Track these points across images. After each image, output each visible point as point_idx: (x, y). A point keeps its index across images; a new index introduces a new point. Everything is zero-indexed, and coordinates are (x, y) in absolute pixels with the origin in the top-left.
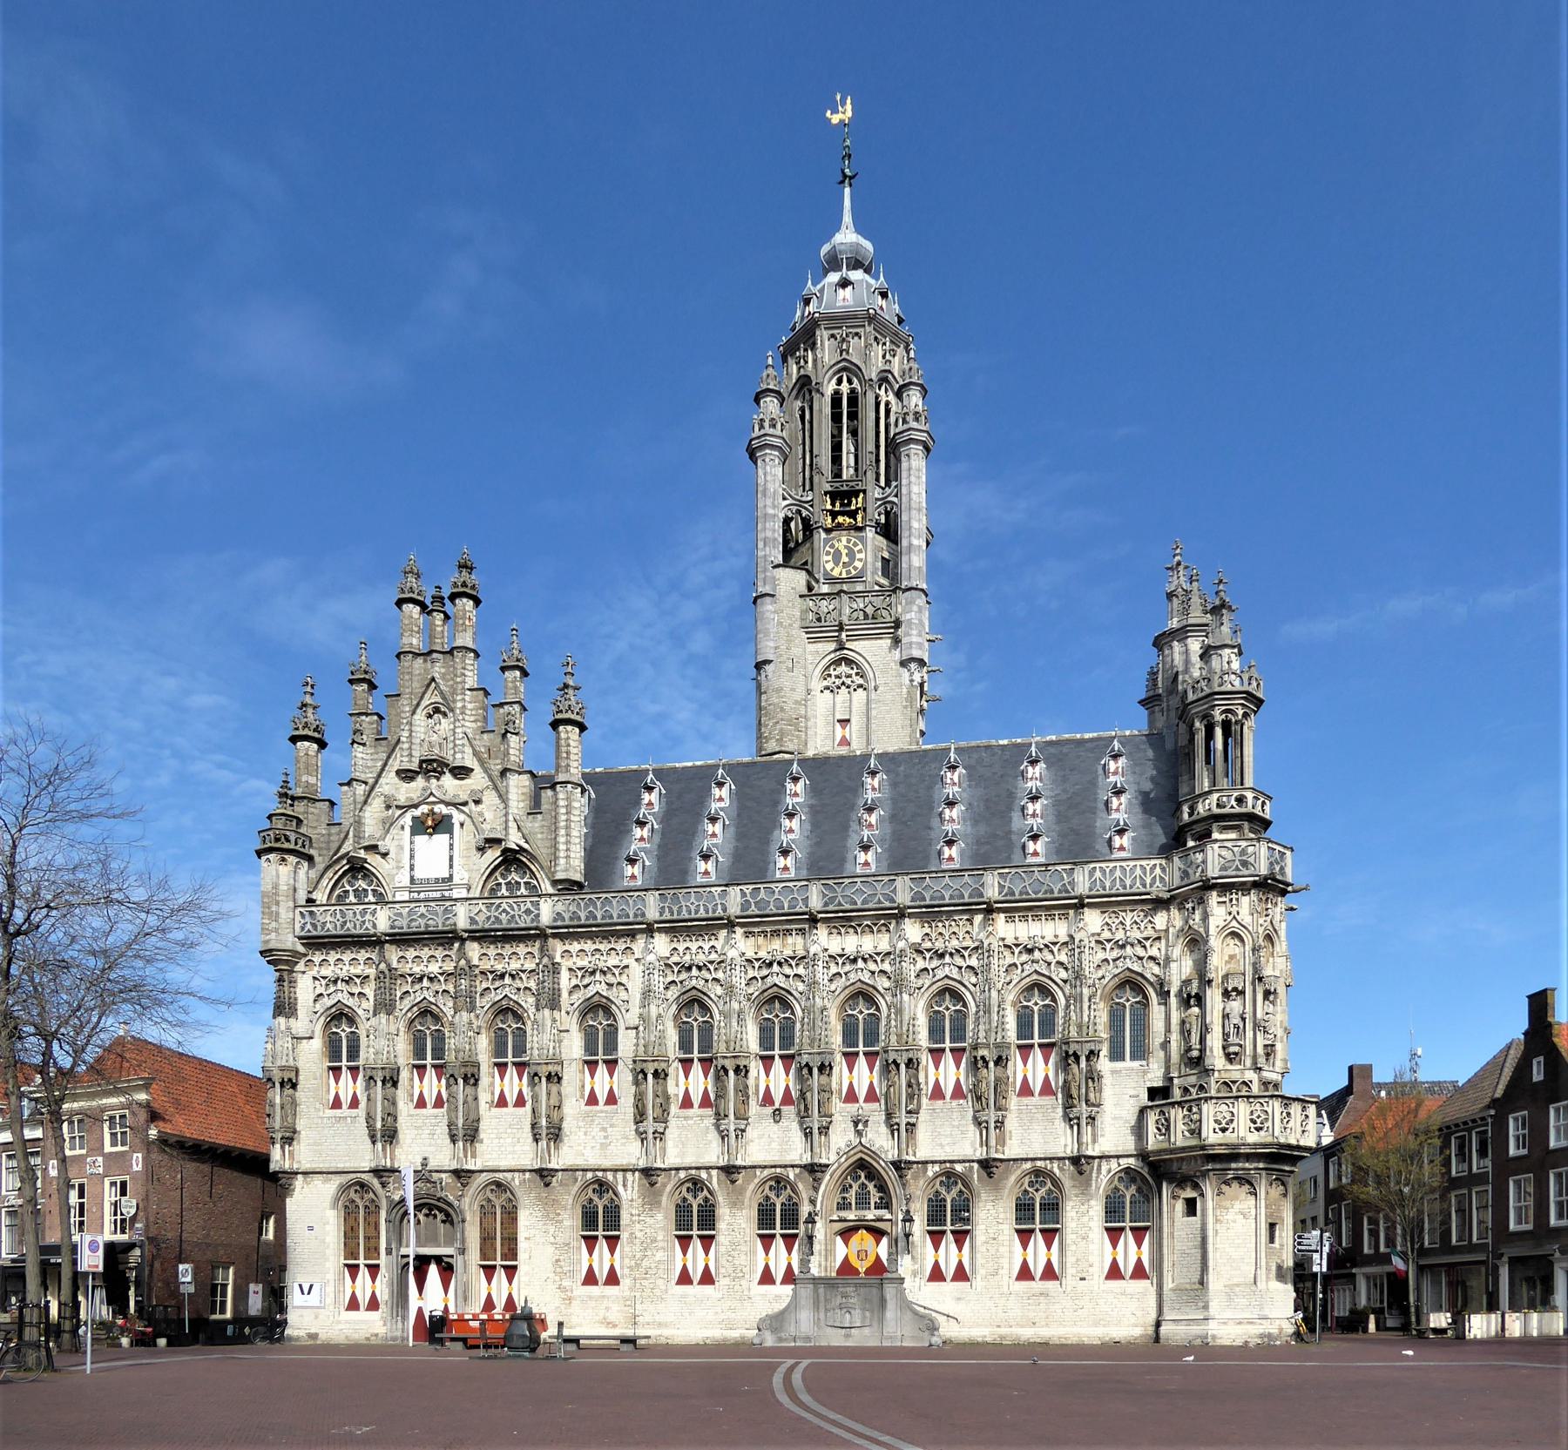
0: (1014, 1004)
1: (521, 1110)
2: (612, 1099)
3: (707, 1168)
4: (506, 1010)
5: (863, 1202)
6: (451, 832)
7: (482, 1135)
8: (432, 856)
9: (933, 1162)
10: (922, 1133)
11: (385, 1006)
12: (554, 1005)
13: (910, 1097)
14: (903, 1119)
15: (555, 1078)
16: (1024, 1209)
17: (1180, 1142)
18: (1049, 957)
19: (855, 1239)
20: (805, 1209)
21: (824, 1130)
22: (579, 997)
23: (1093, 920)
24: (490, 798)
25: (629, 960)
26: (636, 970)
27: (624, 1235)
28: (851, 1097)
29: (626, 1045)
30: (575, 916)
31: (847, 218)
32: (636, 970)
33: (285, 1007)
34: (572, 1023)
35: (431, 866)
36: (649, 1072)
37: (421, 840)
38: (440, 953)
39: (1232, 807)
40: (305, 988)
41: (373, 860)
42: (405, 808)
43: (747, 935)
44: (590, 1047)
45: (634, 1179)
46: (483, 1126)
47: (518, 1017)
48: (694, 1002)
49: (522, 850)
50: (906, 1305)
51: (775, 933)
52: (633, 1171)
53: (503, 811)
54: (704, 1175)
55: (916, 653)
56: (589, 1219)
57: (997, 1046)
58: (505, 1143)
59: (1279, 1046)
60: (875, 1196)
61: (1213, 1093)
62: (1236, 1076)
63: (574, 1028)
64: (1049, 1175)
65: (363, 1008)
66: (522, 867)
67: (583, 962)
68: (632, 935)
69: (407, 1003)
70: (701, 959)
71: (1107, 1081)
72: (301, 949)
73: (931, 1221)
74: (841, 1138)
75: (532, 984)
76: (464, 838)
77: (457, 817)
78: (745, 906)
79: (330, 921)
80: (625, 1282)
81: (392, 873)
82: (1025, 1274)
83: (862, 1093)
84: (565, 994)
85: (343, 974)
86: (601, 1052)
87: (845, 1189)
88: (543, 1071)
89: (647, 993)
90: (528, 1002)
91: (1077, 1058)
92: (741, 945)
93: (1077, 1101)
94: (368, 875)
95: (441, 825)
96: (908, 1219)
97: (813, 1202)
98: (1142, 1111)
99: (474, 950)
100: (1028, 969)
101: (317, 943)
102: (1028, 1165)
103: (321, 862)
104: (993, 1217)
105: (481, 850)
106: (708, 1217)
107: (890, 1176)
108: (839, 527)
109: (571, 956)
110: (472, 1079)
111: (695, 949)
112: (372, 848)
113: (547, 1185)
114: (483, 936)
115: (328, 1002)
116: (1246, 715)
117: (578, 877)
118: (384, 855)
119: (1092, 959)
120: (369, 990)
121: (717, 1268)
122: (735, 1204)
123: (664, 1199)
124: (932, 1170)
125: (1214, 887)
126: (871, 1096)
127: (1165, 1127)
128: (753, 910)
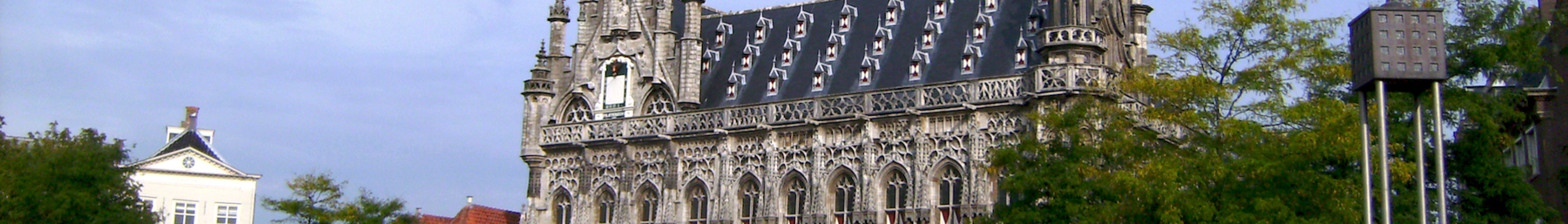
0: (935, 180)
4: (649, 189)
8: (618, 92)
11: (584, 189)
12: (671, 184)
22: (688, 179)
24: (647, 51)
30: (686, 127)
37: (610, 79)
41: (587, 94)
51: (796, 134)
53: (654, 58)
66: (665, 96)
69: (598, 185)
76: (631, 77)
77: (630, 64)
79: (561, 136)
94: (585, 104)
95: (619, 69)
99: (632, 152)
112: (585, 87)
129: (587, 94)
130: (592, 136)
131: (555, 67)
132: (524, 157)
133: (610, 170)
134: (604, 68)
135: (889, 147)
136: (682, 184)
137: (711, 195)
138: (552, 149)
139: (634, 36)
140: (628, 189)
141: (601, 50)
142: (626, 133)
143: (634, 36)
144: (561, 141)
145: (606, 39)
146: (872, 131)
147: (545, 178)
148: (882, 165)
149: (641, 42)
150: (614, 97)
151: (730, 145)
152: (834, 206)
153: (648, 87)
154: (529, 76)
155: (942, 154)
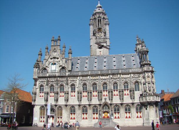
1: (63, 97)
2: (74, 96)
3: (86, 105)
5: (106, 109)
6: (56, 65)
8: (54, 67)
12: (68, 85)
14: (111, 98)
15: (68, 93)
16: (126, 110)
17: (145, 101)
19: (105, 113)
20: (99, 110)
21: (101, 100)
24: (61, 61)
25: (77, 79)
26: (78, 81)
27: (76, 113)
28: (104, 96)
29: (76, 90)
32: (78, 81)
33: (35, 85)
35: (54, 69)
36: (80, 93)
37: (52, 66)
38: (54, 79)
40: (38, 83)
41: (47, 68)
43: (91, 76)
44: (72, 90)
45: (77, 106)
46: (59, 99)
47: (63, 86)
48: (85, 84)
49: (64, 67)
50: (112, 122)
51: (95, 76)
52: (77, 105)
54: (86, 105)
56: (71, 111)
58: (61, 101)
59: (155, 89)
60: (107, 108)
61: (148, 95)
63: (70, 87)
64: (129, 105)
66: (64, 69)
68: (77, 77)
70: (86, 79)
71: (135, 94)
72: (38, 78)
73: (115, 111)
74: (103, 101)
75: (65, 82)
76: (58, 66)
77: (57, 63)
78: (91, 73)
79: (41, 75)
80: (76, 119)
81: (49, 70)
83: (105, 95)
84: (69, 83)
86: (73, 90)
87: (104, 107)
88: (66, 92)
89: (79, 84)
90: (65, 84)
95: (55, 64)
96: (112, 111)
97: (100, 109)
98: (140, 97)
99: (58, 78)
100: (125, 81)
101: (40, 77)
104: (122, 110)
105: (60, 67)
106: (86, 111)
107: (109, 106)
109: (70, 79)
110: (58, 94)
111: (85, 78)
112: (47, 67)
113: (66, 107)
114: (59, 77)
117: (71, 70)
118: (48, 67)
120: (45, 83)
121: (88, 117)
122: (90, 109)
124: (114, 105)
126: (107, 96)
127: (142, 99)
128: (92, 74)
129: (47, 68)
133: (53, 82)
134: (51, 63)
136: (70, 84)
138: (40, 77)
139: (58, 58)
143: (58, 58)
145: (51, 59)
148: (113, 82)
149: (59, 59)
153: (61, 67)
154: (35, 64)
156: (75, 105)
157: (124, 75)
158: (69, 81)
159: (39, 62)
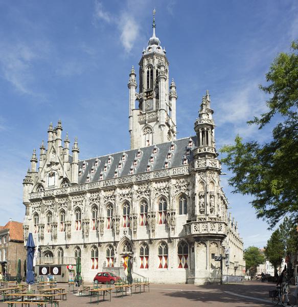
7: (58, 237)
9: (140, 240)
10: (138, 233)
13: (134, 225)
18: (165, 191)
19: (126, 258)
20: (115, 251)
21: (118, 234)
22: (75, 207)
23: (174, 181)
24: (61, 169)
31: (154, 34)
33: (27, 214)
34: (73, 213)
39: (203, 151)
42: (47, 172)
51: (110, 191)
55: (162, 124)
57: (152, 213)
62: (203, 217)
65: (39, 213)
67: (75, 200)
68: (84, 194)
72: (30, 202)
74: (121, 235)
76: (57, 177)
77: (56, 173)
79: (35, 196)
81: (45, 185)
82: (161, 266)
85: (36, 206)
91: (169, 214)
92: (103, 194)
93: (168, 224)
94: (42, 187)
95: (53, 175)
97: (116, 250)
99: (57, 200)
101: (33, 201)
102: (160, 240)
103: (34, 184)
104: (154, 252)
105: (60, 179)
108: (148, 99)
111: (95, 196)
114: (58, 196)
115: (34, 212)
116: (208, 129)
119: (173, 192)
123: (89, 250)
124: (140, 242)
125: (196, 171)
128: (105, 186)
130: (44, 195)
131: (33, 175)
132: (24, 203)
134: (48, 175)
135: (141, 193)
137: (83, 211)
138: (33, 201)
139: (57, 164)
140: (56, 211)
141: (49, 169)
142: (55, 194)
143: (57, 164)
144: (35, 198)
145: (48, 166)
146: (136, 187)
147: (31, 210)
149: (59, 165)
150: (51, 184)
151: (88, 195)
152: (123, 213)
153: (62, 179)
155: (160, 194)
156: (80, 244)
157: (159, 182)
158: (72, 203)
159: (30, 175)
